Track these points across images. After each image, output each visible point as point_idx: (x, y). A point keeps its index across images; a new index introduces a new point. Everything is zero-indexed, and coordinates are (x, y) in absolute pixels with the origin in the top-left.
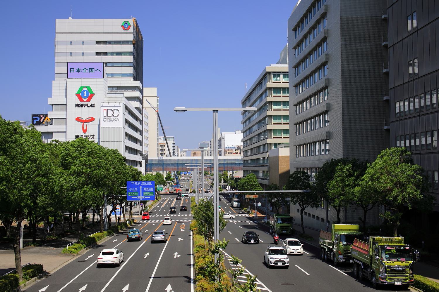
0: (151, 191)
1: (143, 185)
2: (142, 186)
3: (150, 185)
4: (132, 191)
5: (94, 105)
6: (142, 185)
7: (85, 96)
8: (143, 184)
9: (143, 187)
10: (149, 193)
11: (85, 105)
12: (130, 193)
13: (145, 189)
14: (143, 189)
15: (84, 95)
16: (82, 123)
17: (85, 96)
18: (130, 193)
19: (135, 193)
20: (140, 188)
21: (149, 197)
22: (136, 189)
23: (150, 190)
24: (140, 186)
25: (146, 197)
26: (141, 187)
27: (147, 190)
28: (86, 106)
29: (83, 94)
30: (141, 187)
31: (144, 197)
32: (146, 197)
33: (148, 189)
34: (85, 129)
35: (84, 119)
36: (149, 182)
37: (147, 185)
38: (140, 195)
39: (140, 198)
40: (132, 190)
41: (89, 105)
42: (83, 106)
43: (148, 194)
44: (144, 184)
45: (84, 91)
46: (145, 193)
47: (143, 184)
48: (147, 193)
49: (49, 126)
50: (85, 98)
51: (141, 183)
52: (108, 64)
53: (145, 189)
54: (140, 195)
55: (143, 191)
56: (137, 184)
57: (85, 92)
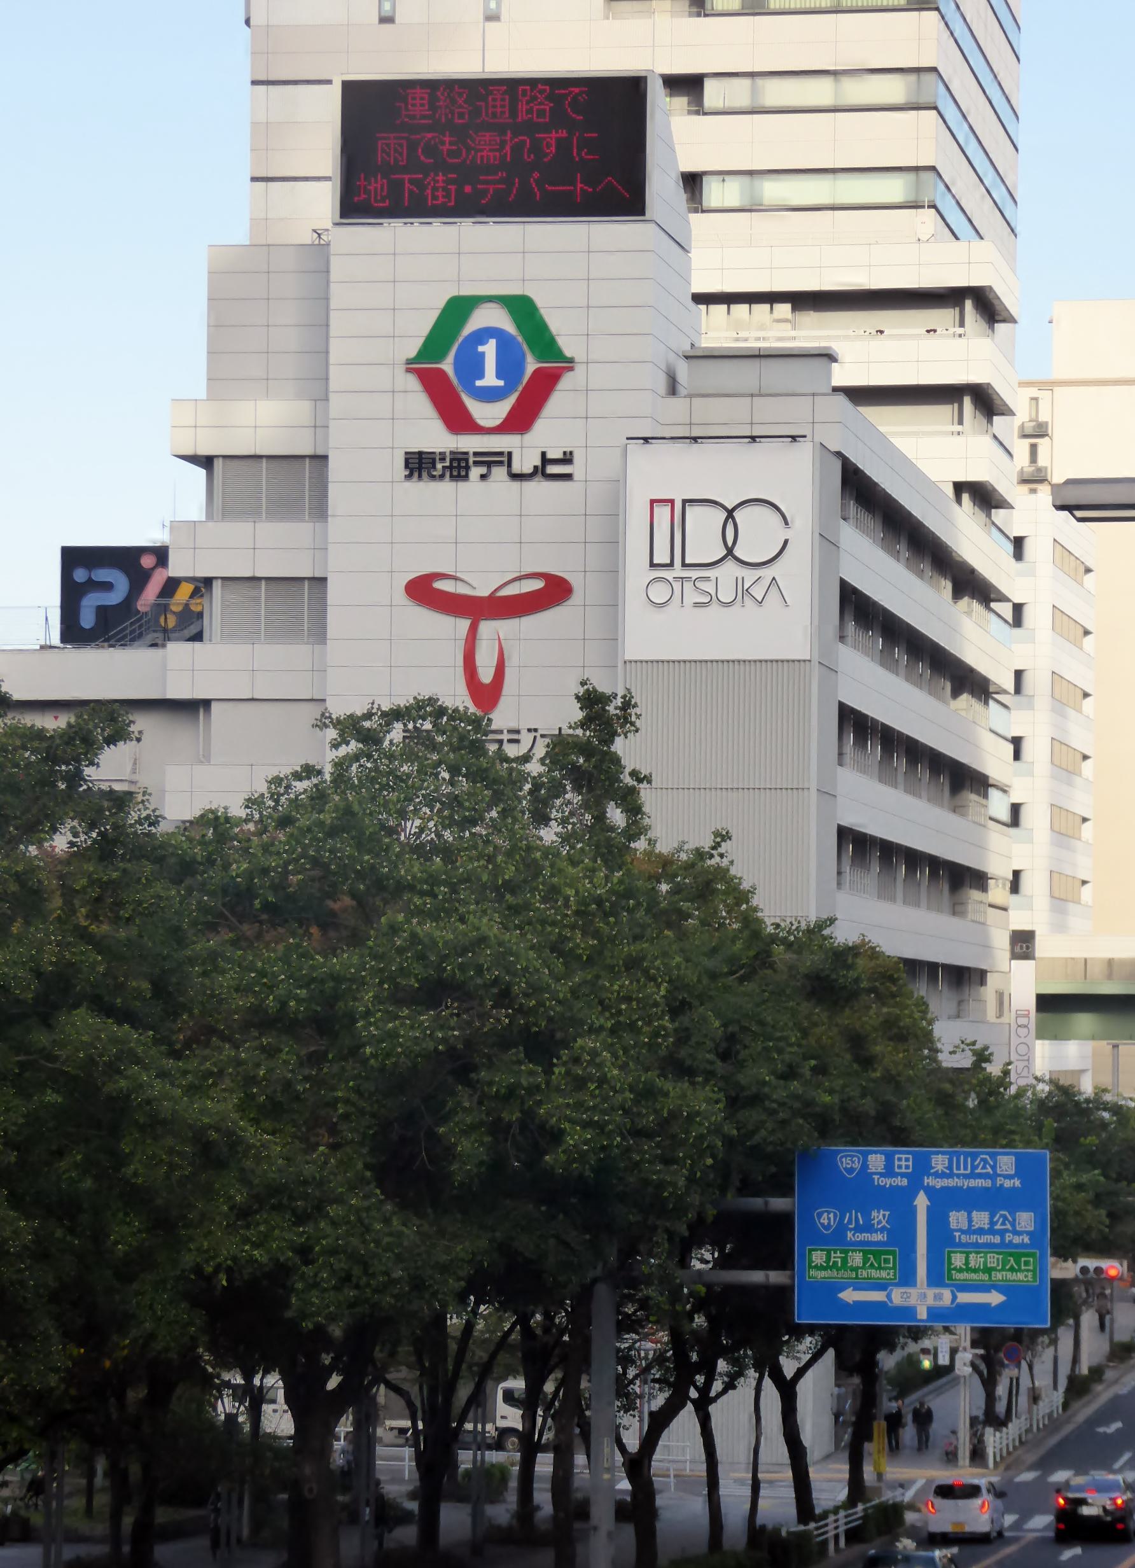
0: (1017, 1240)
1: (939, 1183)
2: (931, 1192)
3: (1008, 1184)
4: (837, 1239)
5: (567, 459)
6: (929, 1181)
7: (490, 379)
8: (943, 1175)
9: (943, 1202)
10: (993, 1260)
11: (491, 461)
12: (818, 1257)
13: (957, 1219)
14: (937, 1220)
15: (481, 376)
16: (464, 624)
17: (490, 379)
18: (818, 1257)
19: (865, 1260)
20: (913, 1211)
21: (995, 1298)
22: (880, 1217)
23: (1002, 1233)
24: (908, 1195)
25: (965, 1298)
26: (922, 1202)
27: (981, 1231)
28: (499, 473)
29: (471, 366)
30: (922, 1202)
31: (947, 1294)
32: (965, 1298)
33: (981, 1218)
34: (486, 675)
35: (484, 592)
36: (993, 1156)
37: (973, 1183)
38: (907, 1278)
39: (931, 1293)
40: (841, 1229)
41: (526, 462)
42: (475, 472)
43: (988, 1270)
44: (951, 1175)
45: (482, 335)
46: (958, 1260)
47: (937, 1175)
48: (975, 1260)
49: (178, 651)
50: (490, 395)
51: (922, 1167)
52: (713, 93)
53: (957, 1219)
54: (907, 1278)
55: (940, 1237)
56: (889, 1172)
57: (489, 350)
